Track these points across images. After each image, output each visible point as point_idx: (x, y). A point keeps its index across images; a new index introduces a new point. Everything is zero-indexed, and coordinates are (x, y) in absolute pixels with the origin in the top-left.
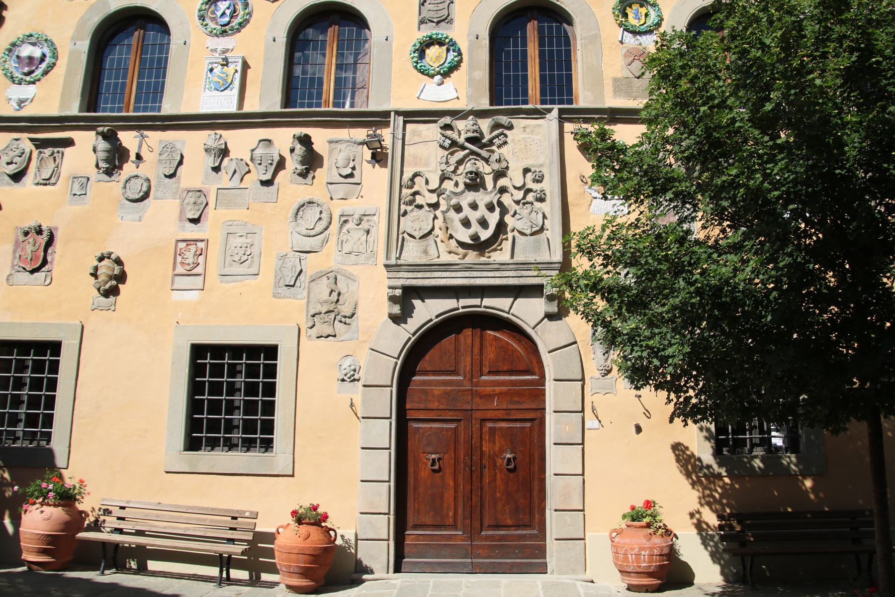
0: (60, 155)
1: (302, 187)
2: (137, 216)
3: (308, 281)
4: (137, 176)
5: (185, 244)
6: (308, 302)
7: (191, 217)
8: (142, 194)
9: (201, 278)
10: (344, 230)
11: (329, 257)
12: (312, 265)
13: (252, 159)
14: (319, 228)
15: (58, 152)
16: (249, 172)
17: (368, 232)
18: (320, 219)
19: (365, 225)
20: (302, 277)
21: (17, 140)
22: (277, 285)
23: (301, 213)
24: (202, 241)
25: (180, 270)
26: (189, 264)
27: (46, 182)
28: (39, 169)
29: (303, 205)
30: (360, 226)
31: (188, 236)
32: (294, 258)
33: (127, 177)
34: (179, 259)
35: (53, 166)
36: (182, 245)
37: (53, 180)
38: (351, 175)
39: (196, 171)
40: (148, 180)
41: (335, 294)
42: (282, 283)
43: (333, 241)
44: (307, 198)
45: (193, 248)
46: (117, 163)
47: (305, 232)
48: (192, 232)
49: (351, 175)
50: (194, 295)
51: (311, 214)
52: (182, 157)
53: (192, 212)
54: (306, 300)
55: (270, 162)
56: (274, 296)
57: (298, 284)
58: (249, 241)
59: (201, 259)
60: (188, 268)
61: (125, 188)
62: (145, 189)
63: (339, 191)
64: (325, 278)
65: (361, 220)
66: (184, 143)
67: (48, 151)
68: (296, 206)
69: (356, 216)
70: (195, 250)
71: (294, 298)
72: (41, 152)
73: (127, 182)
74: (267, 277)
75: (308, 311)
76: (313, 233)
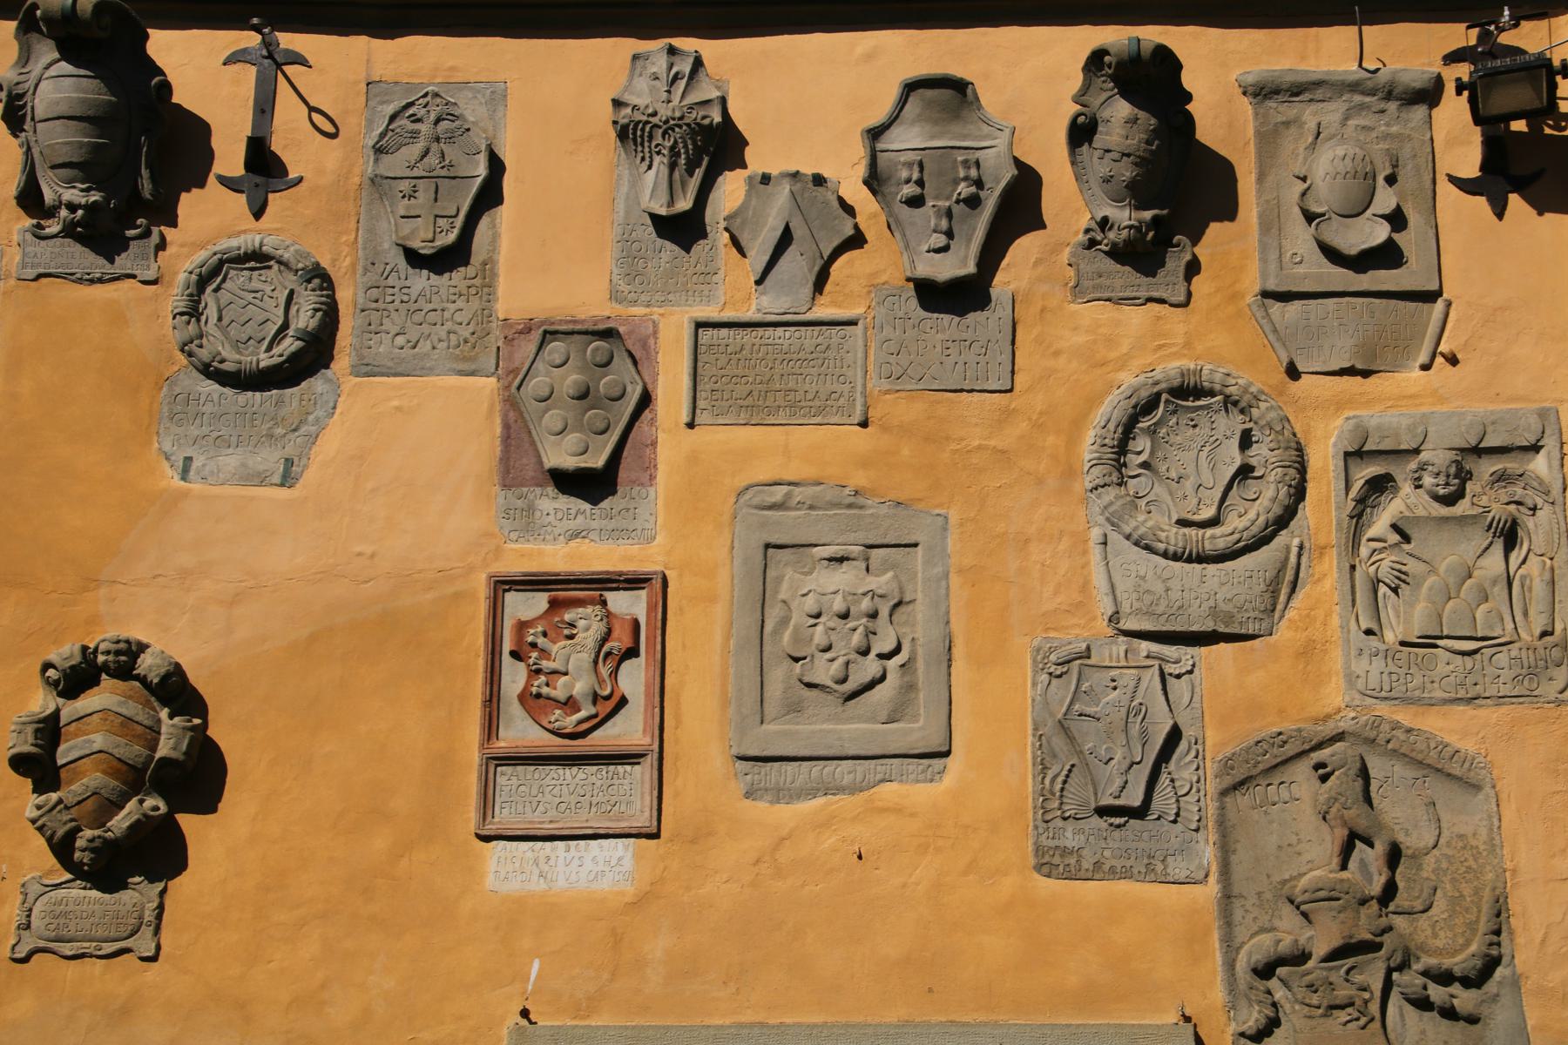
1: (1136, 318)
2: (269, 459)
3: (1212, 786)
4: (257, 258)
5: (536, 603)
6: (1227, 896)
7: (569, 462)
8: (289, 345)
9: (640, 774)
10: (1380, 525)
11: (1318, 663)
12: (1228, 697)
13: (875, 181)
14: (1245, 518)
16: (856, 240)
17: (1510, 536)
18: (1245, 472)
19: (1484, 498)
20: (1181, 769)
22: (1051, 805)
23: (1142, 443)
24: (634, 582)
25: (520, 731)
26: (570, 704)
29: (1150, 406)
30: (1463, 507)
31: (557, 557)
32: (1127, 675)
34: (514, 678)
36: (526, 606)
38: (1388, 256)
39: (564, 242)
40: (319, 277)
41: (1370, 857)
42: (1079, 795)
43: (1325, 580)
44: (1170, 368)
45: (587, 622)
46: (146, 187)
47: (1175, 537)
48: (569, 540)
49: (1388, 256)
50: (603, 868)
51: (1198, 455)
52: (496, 166)
53: (573, 439)
54: (1213, 887)
55: (964, 189)
56: (1045, 867)
57: (1163, 800)
58: (881, 582)
59: (633, 679)
60: (569, 722)
61: (193, 311)
62: (305, 318)
63: (1338, 330)
64: (1302, 772)
65: (1464, 476)
66: (497, 97)
68: (1110, 409)
69: (1437, 456)
70: (597, 628)
71: (1151, 874)
73: (203, 282)
74: (994, 762)
75: (1230, 947)
76: (1216, 538)
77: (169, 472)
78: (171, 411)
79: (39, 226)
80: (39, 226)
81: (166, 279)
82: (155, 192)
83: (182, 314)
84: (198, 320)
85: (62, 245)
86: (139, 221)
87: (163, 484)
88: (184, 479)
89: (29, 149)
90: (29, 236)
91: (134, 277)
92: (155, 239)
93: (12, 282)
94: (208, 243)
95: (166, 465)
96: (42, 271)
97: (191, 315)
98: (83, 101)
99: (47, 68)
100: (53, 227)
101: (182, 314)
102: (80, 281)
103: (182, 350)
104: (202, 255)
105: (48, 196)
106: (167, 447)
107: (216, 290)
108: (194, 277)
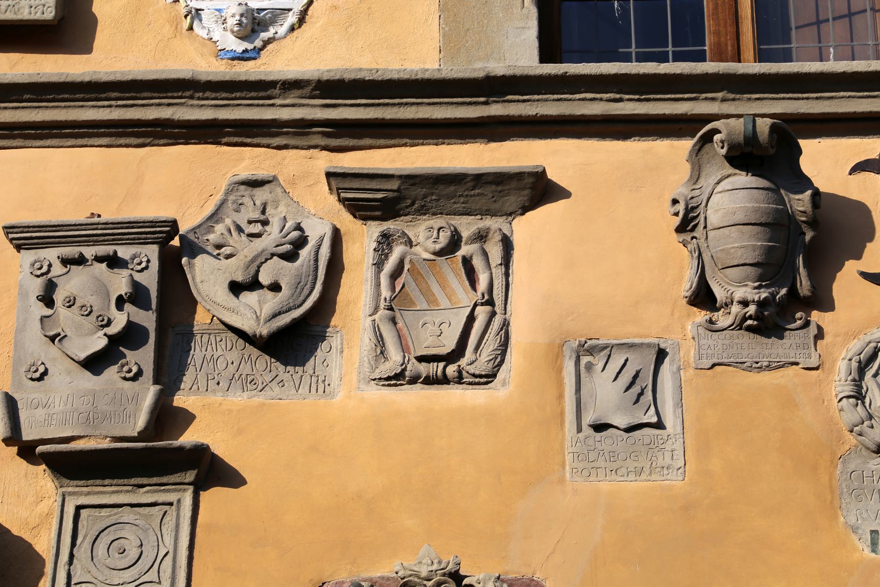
0: (495, 252)
15: (481, 237)
21: (255, 184)
27: (442, 368)
28: (395, 306)
33: (855, 346)
35: (465, 298)
37: (475, 360)
46: (804, 286)
61: (859, 395)
67: (424, 233)
72: (386, 241)
73: (862, 369)
77: (860, 546)
78: (848, 487)
79: (711, 322)
80: (711, 322)
81: (827, 366)
82: (813, 286)
83: (848, 397)
84: (863, 403)
85: (731, 337)
86: (798, 315)
87: (857, 556)
88: (874, 551)
89: (700, 254)
90: (701, 330)
91: (797, 364)
92: (813, 330)
93: (691, 371)
94: (859, 333)
95: (854, 538)
96: (716, 361)
97: (857, 398)
98: (756, 210)
99: (718, 183)
100: (723, 320)
101: (848, 397)
102: (750, 369)
103: (851, 431)
104: (855, 346)
105: (720, 294)
106: (852, 520)
107: (875, 376)
108: (854, 364)
